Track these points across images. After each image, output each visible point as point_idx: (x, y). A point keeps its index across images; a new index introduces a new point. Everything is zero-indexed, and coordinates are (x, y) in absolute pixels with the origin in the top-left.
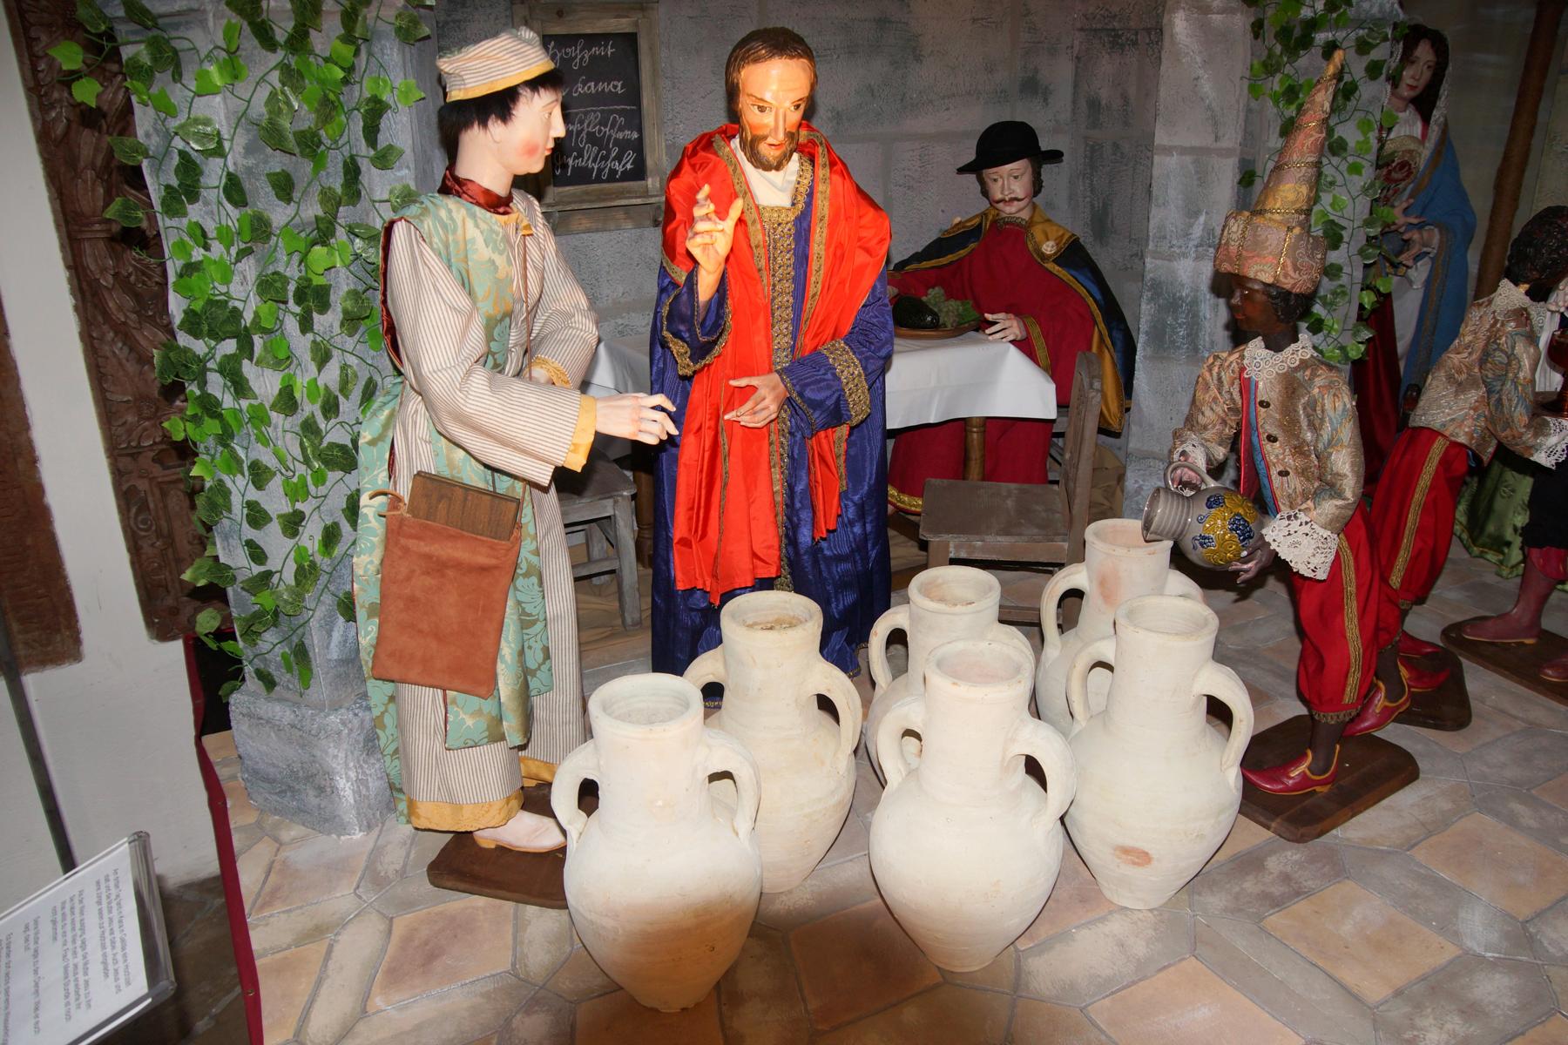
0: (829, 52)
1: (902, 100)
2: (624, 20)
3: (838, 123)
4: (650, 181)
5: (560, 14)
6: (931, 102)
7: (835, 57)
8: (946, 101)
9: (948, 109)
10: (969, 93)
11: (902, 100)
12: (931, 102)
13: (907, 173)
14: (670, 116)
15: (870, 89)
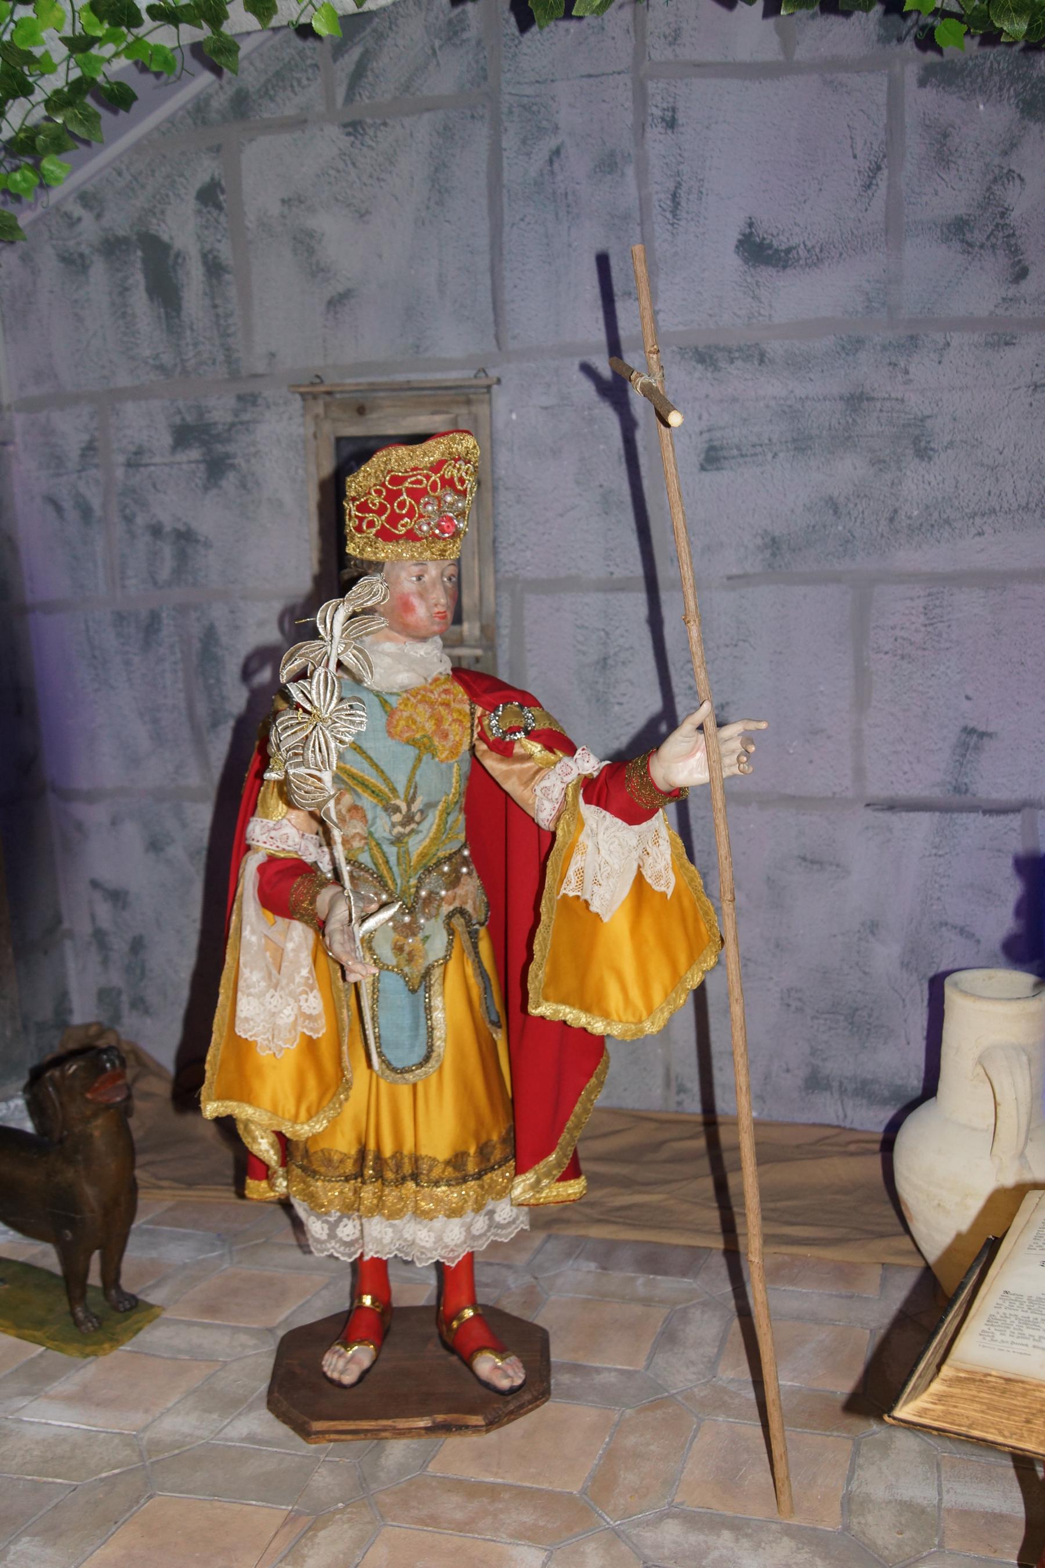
0: (759, 449)
1: (891, 520)
2: (438, 418)
3: (774, 555)
4: (466, 626)
5: (361, 411)
6: (947, 521)
7: (769, 456)
8: (978, 520)
9: (980, 534)
10: (1026, 508)
11: (891, 520)
12: (947, 521)
13: (899, 633)
14: (512, 541)
15: (834, 506)
